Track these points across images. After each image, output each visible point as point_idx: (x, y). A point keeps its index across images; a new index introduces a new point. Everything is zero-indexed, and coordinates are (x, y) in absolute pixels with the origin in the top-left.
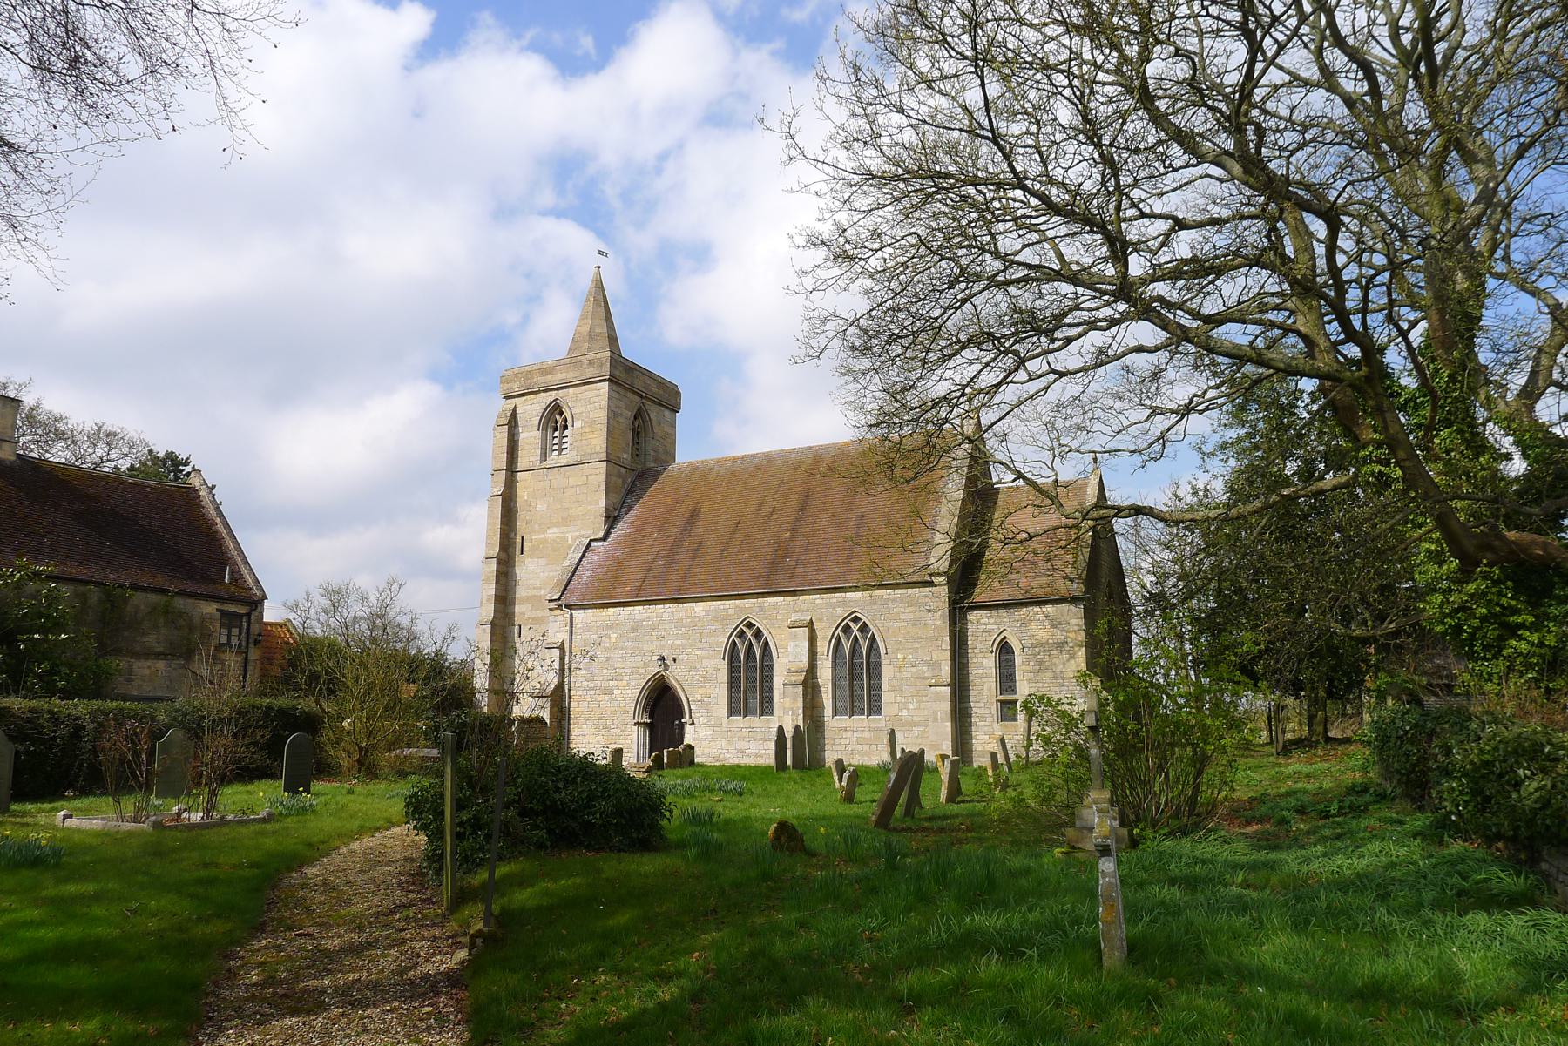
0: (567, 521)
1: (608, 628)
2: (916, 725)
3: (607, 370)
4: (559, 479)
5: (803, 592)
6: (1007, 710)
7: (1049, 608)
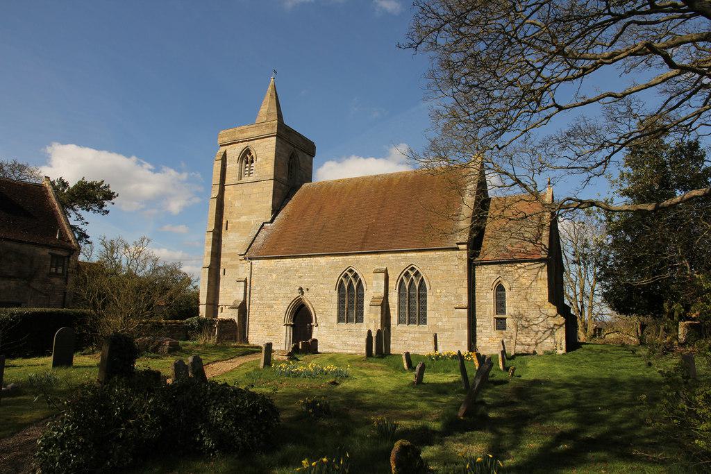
0: (251, 212)
1: (271, 271)
2: (447, 330)
3: (275, 130)
4: (247, 189)
6: (500, 324)
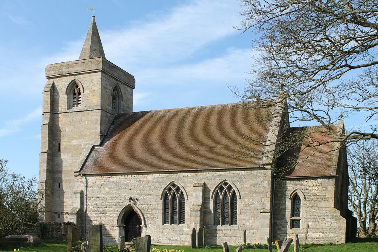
0: (81, 137)
2: (253, 229)
3: (100, 66)
5: (201, 171)
7: (319, 181)
